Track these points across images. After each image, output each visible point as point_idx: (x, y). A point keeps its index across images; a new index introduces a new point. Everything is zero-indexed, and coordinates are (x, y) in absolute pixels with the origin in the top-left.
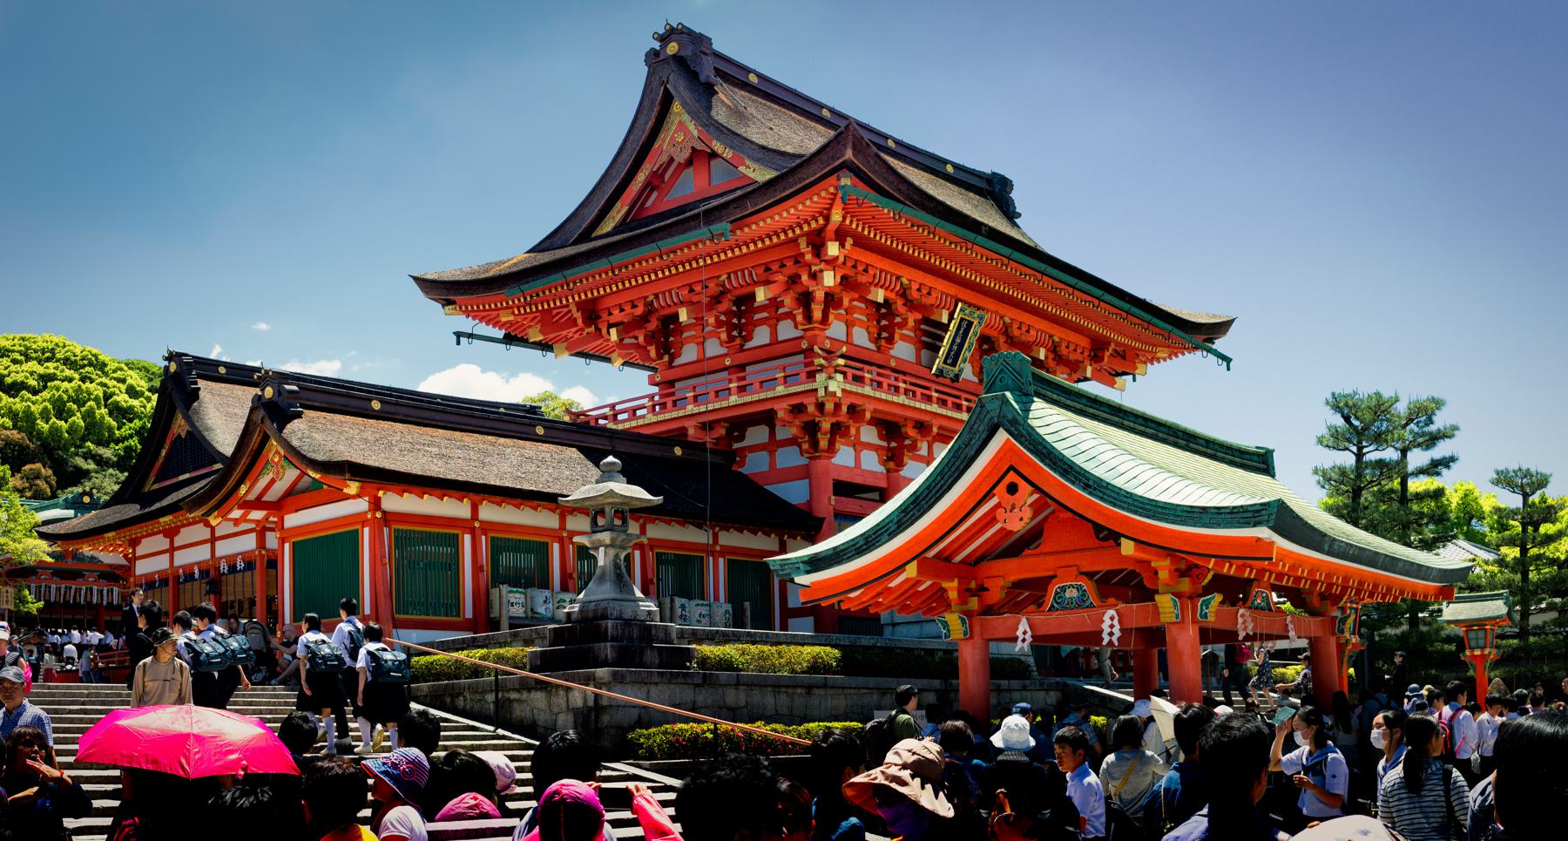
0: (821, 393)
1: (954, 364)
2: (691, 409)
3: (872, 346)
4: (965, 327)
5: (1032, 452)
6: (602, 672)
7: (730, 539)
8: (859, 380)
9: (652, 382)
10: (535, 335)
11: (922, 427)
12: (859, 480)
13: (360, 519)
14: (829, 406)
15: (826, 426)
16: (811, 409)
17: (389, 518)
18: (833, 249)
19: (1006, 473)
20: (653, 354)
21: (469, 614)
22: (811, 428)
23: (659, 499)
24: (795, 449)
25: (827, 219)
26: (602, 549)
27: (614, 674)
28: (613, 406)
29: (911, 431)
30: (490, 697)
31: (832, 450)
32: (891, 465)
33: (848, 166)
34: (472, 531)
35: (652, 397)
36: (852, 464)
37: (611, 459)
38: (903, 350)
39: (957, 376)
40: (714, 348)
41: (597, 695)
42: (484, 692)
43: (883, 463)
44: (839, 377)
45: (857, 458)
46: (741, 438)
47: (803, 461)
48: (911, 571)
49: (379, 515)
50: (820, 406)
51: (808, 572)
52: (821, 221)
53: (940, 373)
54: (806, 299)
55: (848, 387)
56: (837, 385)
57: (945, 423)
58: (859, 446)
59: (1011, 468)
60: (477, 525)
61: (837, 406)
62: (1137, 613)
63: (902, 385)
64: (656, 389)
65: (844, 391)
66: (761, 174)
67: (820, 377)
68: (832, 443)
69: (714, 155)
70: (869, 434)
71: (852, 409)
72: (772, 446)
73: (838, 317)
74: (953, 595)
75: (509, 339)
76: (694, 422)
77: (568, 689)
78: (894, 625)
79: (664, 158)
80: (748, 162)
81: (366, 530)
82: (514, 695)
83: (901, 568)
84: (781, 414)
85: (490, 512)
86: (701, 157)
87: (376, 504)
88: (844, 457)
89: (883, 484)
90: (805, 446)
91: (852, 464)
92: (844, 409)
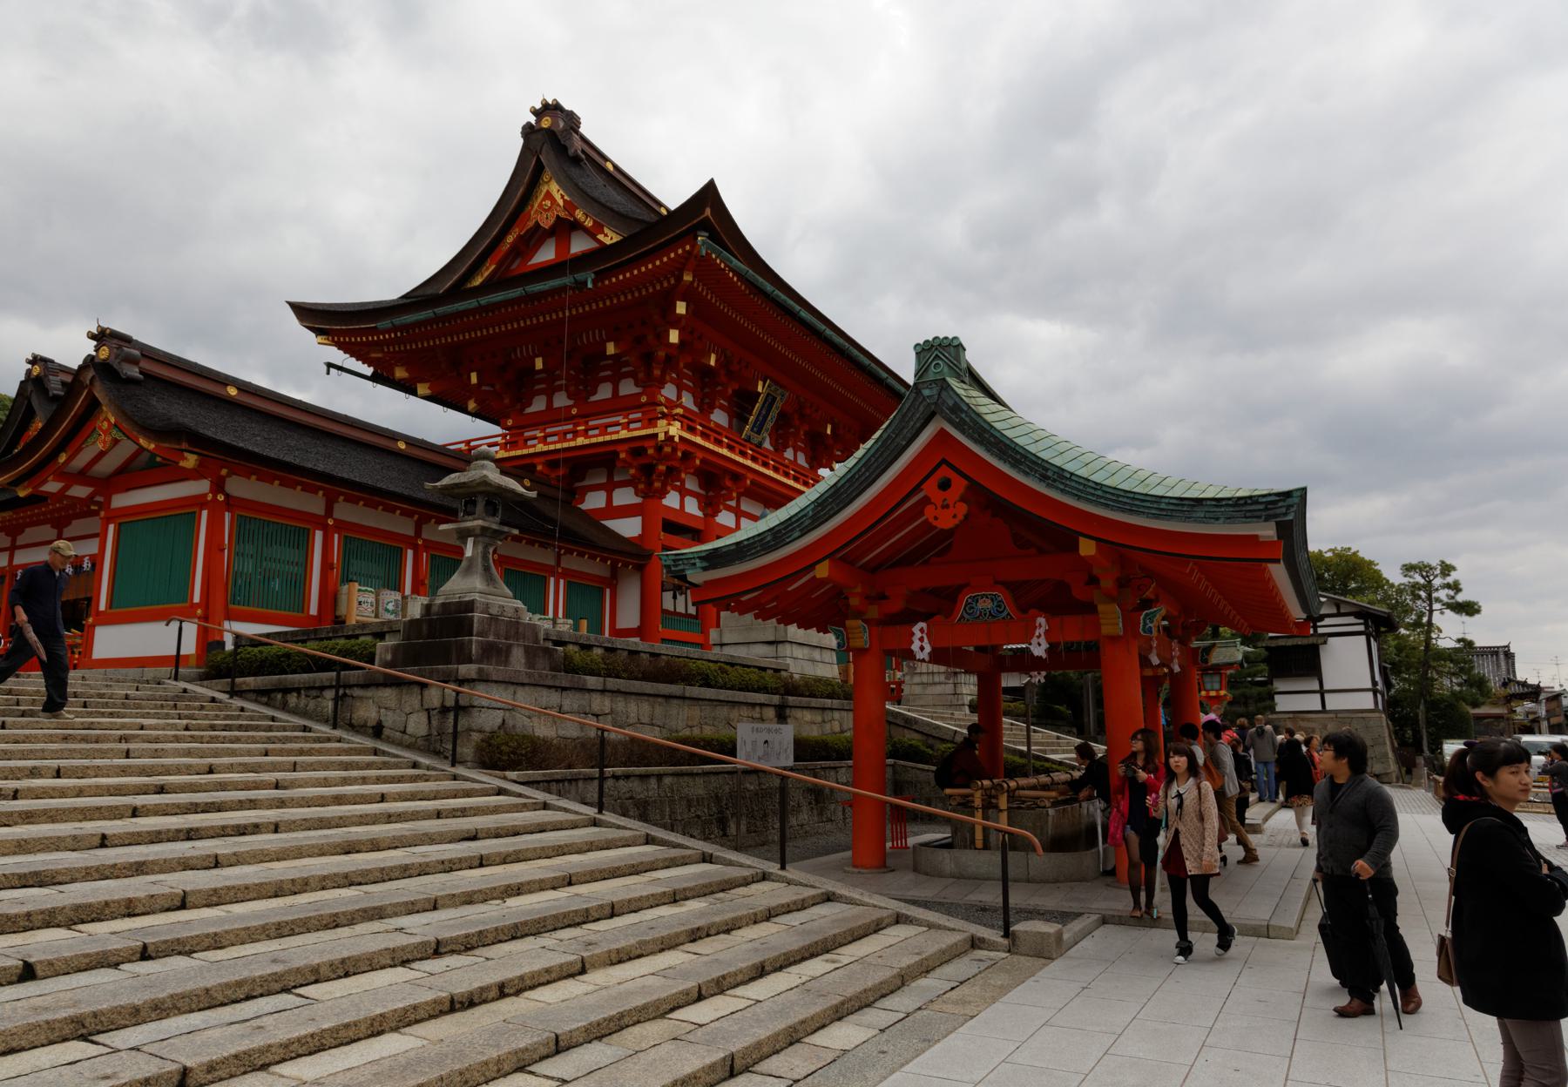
0: (661, 437)
1: (759, 432)
2: (541, 448)
4: (770, 400)
5: (976, 441)
6: (466, 670)
7: (572, 563)
8: (692, 430)
10: (400, 373)
12: (682, 521)
13: (198, 502)
14: (668, 449)
15: (662, 468)
16: (650, 451)
17: (231, 503)
18: (681, 308)
19: (937, 468)
20: (507, 401)
21: (313, 611)
22: (648, 470)
23: (533, 494)
24: (631, 490)
25: (679, 279)
26: (470, 541)
27: (480, 671)
28: (468, 442)
29: (728, 483)
30: (330, 694)
31: (663, 493)
32: (709, 511)
33: (705, 225)
35: (504, 436)
36: (677, 506)
38: (719, 417)
41: (458, 693)
42: (322, 688)
43: (700, 508)
44: (678, 424)
45: (681, 503)
46: (583, 479)
47: (639, 500)
48: (822, 571)
49: (221, 498)
50: (659, 449)
51: (705, 569)
53: (748, 440)
54: (648, 358)
55: (686, 435)
56: (675, 430)
57: (757, 478)
58: (684, 492)
59: (944, 461)
60: (330, 522)
61: (675, 450)
62: (1074, 631)
65: (681, 438)
67: (662, 423)
68: (664, 485)
69: (576, 226)
70: (691, 484)
71: (687, 456)
72: (610, 488)
73: (672, 381)
74: (854, 602)
75: (374, 378)
76: (542, 459)
77: (423, 686)
78: (722, 645)
79: (531, 224)
81: (205, 513)
82: (357, 692)
83: (812, 567)
84: (622, 456)
85: (345, 512)
86: (564, 228)
87: (218, 486)
88: (672, 500)
89: (701, 527)
90: (641, 486)
91: (677, 506)
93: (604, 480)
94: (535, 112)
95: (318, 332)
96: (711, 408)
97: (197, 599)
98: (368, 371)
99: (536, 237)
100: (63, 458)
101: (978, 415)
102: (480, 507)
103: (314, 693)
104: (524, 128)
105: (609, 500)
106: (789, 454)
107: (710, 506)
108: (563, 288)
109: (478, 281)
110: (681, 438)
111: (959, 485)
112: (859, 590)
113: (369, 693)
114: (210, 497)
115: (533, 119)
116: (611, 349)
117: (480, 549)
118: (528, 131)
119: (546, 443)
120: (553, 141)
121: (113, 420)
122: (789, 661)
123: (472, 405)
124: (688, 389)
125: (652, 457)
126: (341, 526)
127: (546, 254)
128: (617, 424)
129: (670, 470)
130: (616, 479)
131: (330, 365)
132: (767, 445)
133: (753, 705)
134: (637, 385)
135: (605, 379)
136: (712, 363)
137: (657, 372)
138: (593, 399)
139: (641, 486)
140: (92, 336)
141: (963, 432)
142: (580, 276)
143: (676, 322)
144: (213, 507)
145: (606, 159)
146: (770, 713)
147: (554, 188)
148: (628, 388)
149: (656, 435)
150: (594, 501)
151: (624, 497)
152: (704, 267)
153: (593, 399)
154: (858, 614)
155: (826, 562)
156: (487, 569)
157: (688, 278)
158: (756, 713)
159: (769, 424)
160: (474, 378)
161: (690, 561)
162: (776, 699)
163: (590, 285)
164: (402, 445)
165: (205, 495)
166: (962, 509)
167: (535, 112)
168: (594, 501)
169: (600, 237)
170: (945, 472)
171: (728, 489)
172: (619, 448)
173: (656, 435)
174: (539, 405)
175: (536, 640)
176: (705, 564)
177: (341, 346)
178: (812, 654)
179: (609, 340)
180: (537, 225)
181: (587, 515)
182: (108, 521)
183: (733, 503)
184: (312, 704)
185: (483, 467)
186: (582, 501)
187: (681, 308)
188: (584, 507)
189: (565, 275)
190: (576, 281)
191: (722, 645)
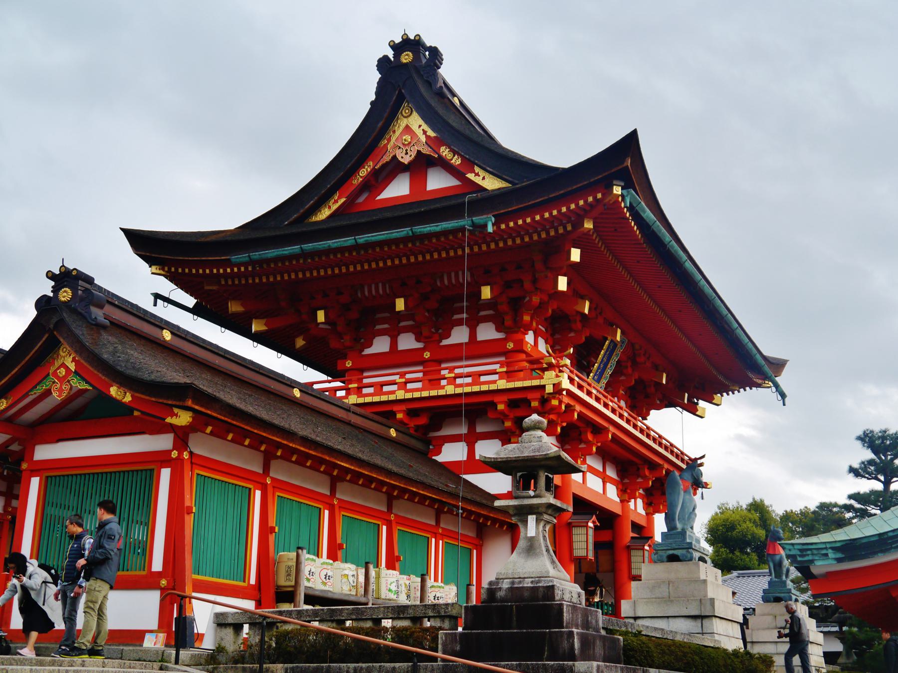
0: (549, 389)
2: (401, 395)
10: (234, 307)
11: (598, 430)
13: (161, 459)
18: (575, 255)
21: (253, 581)
26: (532, 519)
29: (590, 437)
34: (264, 489)
37: (535, 417)
40: (407, 342)
46: (439, 429)
49: (186, 455)
51: (839, 560)
52: (569, 228)
60: (269, 481)
63: (594, 391)
66: (491, 183)
72: (471, 440)
75: (196, 311)
76: (404, 407)
78: (635, 618)
79: (387, 158)
80: (477, 169)
81: (165, 474)
93: (463, 430)
94: (394, 47)
95: (150, 261)
97: (157, 565)
98: (190, 301)
99: (395, 168)
104: (380, 61)
105: (471, 452)
108: (462, 229)
109: (324, 214)
110: (568, 391)
114: (175, 454)
115: (390, 54)
118: (383, 64)
119: (407, 391)
120: (410, 74)
121: (72, 367)
123: (300, 343)
126: (280, 485)
127: (399, 189)
128: (494, 372)
130: (480, 429)
131: (157, 296)
134: (498, 330)
135: (459, 323)
136: (586, 311)
137: (527, 318)
138: (445, 342)
140: (51, 276)
142: (477, 219)
144: (177, 466)
145: (454, 95)
147: (416, 122)
148: (487, 332)
149: (543, 387)
150: (452, 453)
152: (608, 213)
153: (445, 342)
156: (548, 551)
157: (588, 225)
160: (321, 316)
161: (821, 551)
163: (490, 229)
164: (297, 393)
165: (170, 452)
167: (394, 47)
168: (452, 453)
169: (471, 176)
171: (587, 442)
173: (543, 387)
174: (381, 345)
176: (839, 555)
177: (173, 278)
180: (394, 157)
181: (443, 466)
182: (34, 472)
186: (439, 452)
187: (575, 255)
188: (440, 458)
189: (461, 216)
190: (474, 225)
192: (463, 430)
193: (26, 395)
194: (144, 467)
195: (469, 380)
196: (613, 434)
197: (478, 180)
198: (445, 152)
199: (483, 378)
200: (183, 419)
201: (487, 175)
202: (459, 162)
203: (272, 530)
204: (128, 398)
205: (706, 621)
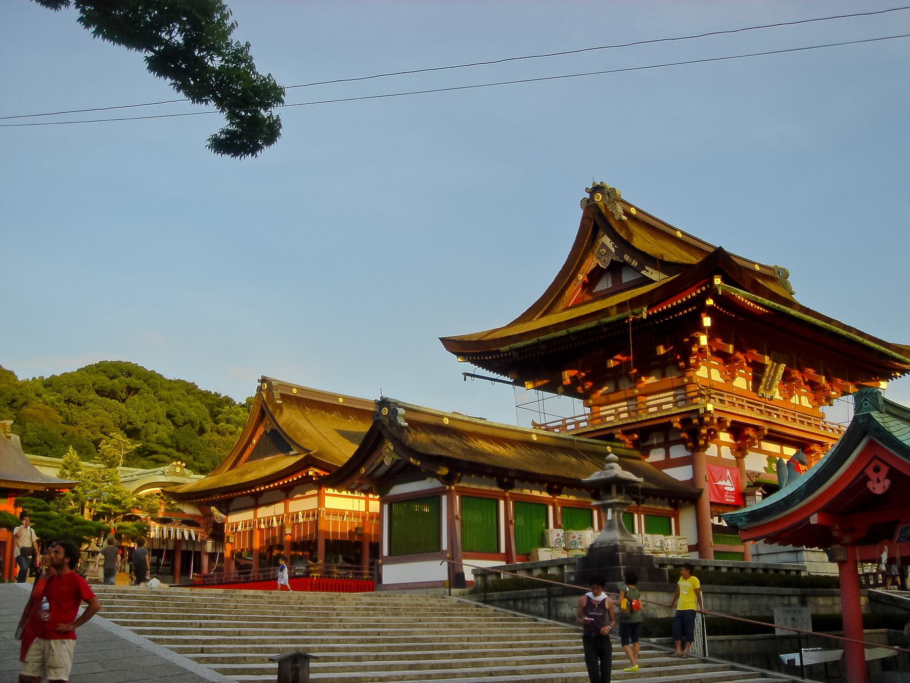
3: (722, 380)
5: (890, 447)
9: (586, 405)
11: (757, 428)
14: (707, 419)
15: (704, 431)
22: (694, 434)
26: (610, 511)
32: (739, 454)
39: (772, 397)
43: (732, 453)
47: (688, 454)
50: (701, 419)
59: (875, 457)
61: (712, 418)
64: (588, 410)
65: (715, 410)
68: (706, 441)
69: (626, 264)
70: (725, 437)
74: (835, 534)
78: (758, 555)
81: (444, 498)
92: (715, 421)
93: (662, 440)
95: (458, 354)
96: (733, 378)
100: (363, 470)
101: (890, 433)
102: (614, 490)
103: (532, 600)
105: (667, 454)
106: (795, 400)
107: (740, 451)
110: (715, 410)
111: (885, 470)
112: (837, 527)
113: (565, 600)
115: (588, 196)
116: (661, 350)
117: (616, 514)
122: (806, 564)
124: (715, 367)
125: (696, 425)
129: (709, 431)
130: (672, 438)
132: (777, 396)
133: (784, 596)
139: (690, 444)
141: (881, 441)
143: (702, 330)
146: (795, 600)
147: (606, 240)
149: (698, 410)
151: (678, 452)
154: (838, 541)
155: (816, 515)
156: (620, 526)
158: (786, 601)
159: (777, 382)
162: (798, 591)
166: (887, 483)
169: (643, 272)
170: (876, 463)
172: (673, 420)
173: (698, 410)
175: (653, 566)
177: (472, 362)
178: (817, 563)
179: (659, 344)
183: (756, 447)
184: (532, 607)
185: (612, 468)
187: (707, 322)
191: (758, 555)
192: (662, 440)
193: (373, 464)
194: (432, 498)
195: (655, 409)
196: (769, 431)
197: (648, 275)
198: (627, 258)
199: (664, 407)
200: (444, 471)
201: (653, 271)
202: (636, 264)
203: (511, 522)
204: (419, 463)
205: (799, 554)
